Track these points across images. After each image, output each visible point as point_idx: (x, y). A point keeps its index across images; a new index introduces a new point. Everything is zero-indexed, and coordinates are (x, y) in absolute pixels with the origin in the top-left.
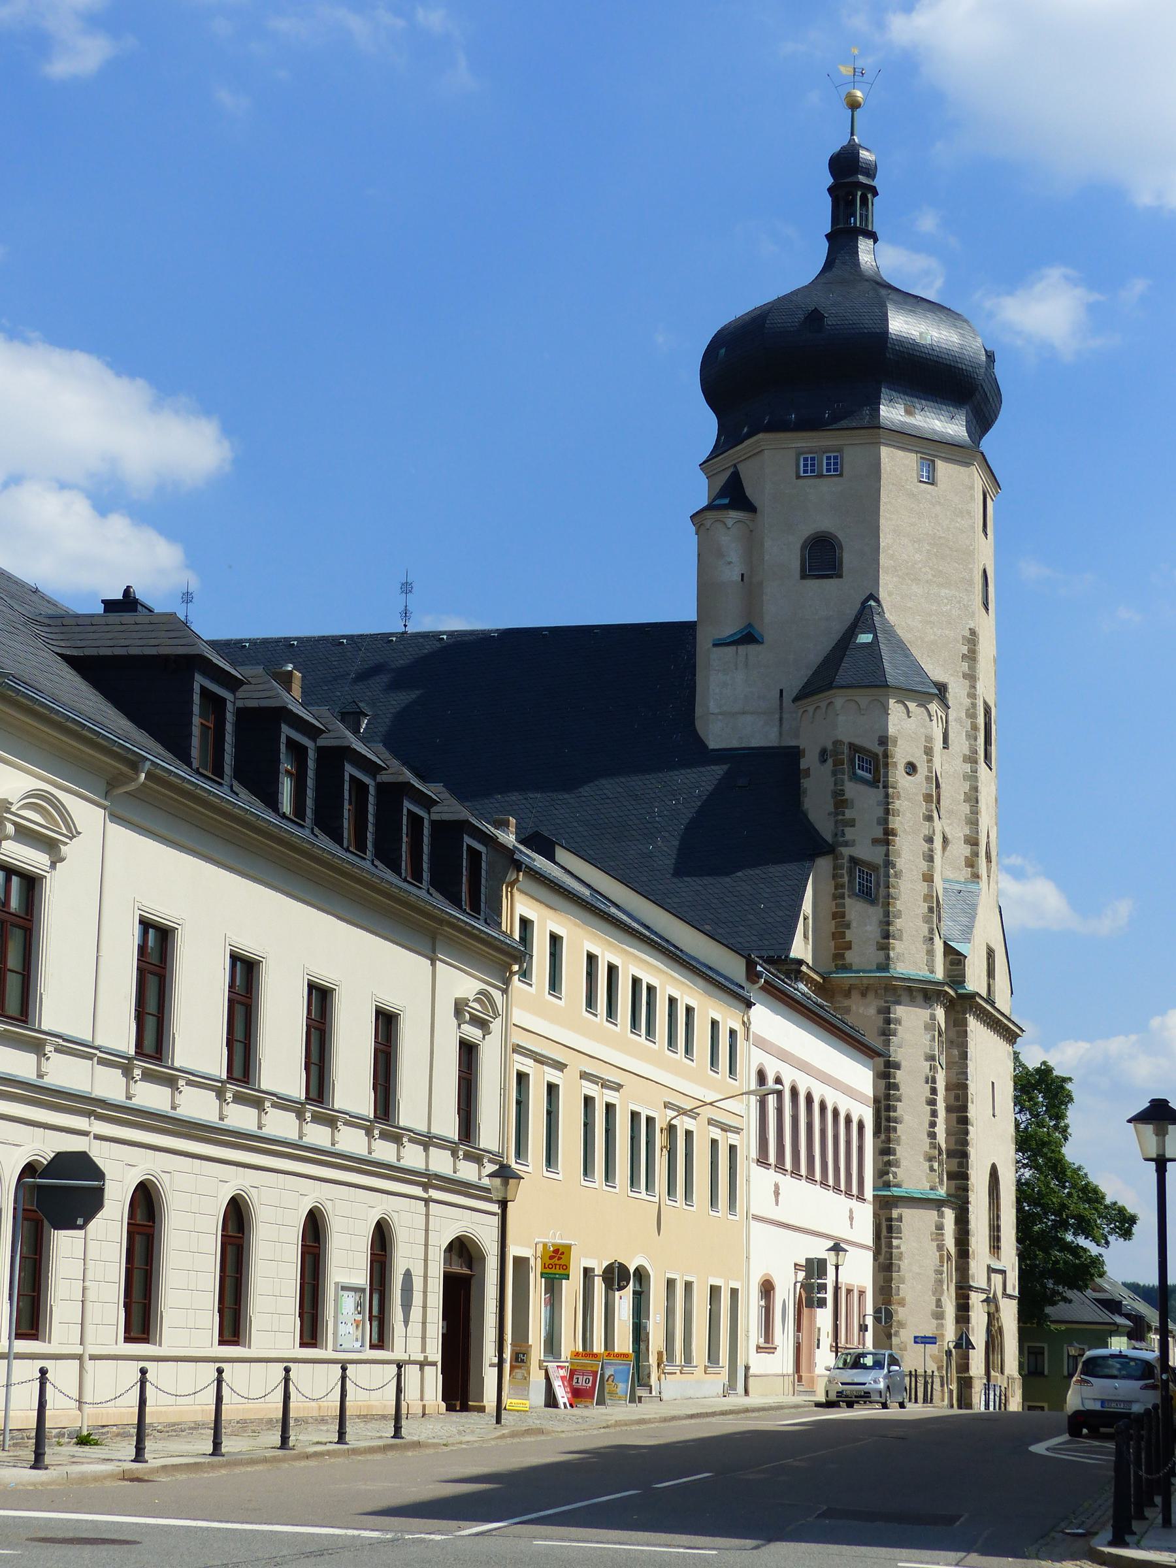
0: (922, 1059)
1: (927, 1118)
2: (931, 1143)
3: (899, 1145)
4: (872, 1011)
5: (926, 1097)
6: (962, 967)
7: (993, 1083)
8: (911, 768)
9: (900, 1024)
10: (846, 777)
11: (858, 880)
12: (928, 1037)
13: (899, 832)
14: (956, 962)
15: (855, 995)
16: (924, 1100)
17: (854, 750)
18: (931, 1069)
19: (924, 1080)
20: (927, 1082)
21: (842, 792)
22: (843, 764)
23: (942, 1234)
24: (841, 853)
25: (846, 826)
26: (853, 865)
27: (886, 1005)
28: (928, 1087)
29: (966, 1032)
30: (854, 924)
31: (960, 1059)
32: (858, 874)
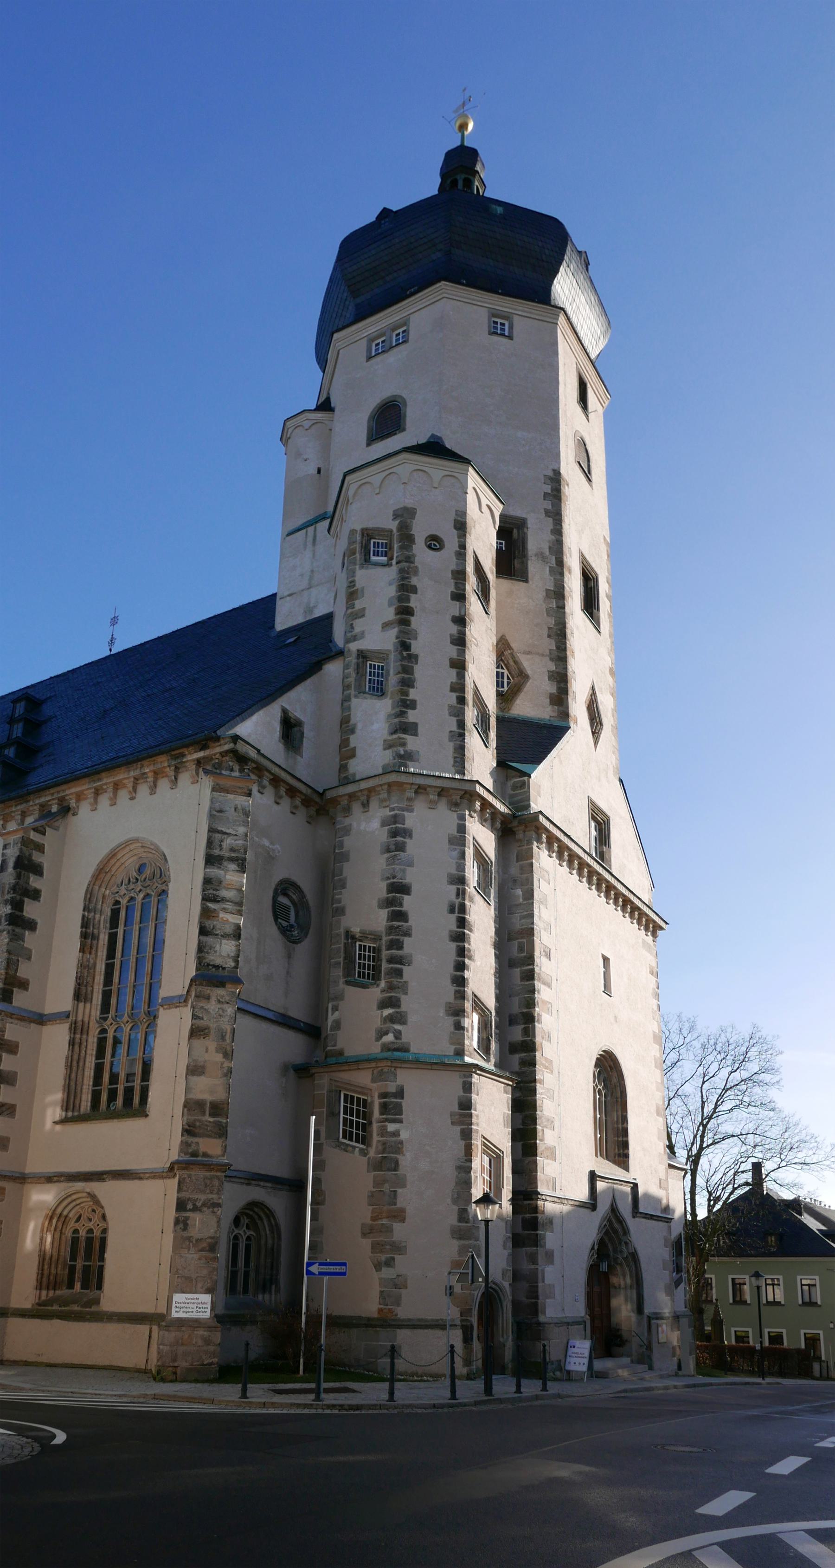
0: (445, 880)
1: (452, 957)
2: (456, 992)
3: (406, 994)
4: (375, 824)
5: (450, 931)
6: (526, 789)
7: (606, 960)
8: (435, 543)
9: (411, 836)
10: (357, 567)
11: (368, 677)
12: (455, 854)
13: (417, 611)
14: (519, 785)
15: (356, 807)
16: (446, 934)
17: (368, 535)
18: (458, 895)
19: (446, 908)
20: (452, 910)
21: (352, 584)
22: (354, 553)
23: (471, 1115)
24: (349, 650)
25: (356, 619)
26: (361, 660)
27: (392, 813)
28: (453, 918)
29: (531, 865)
30: (359, 726)
31: (524, 899)
32: (368, 670)
